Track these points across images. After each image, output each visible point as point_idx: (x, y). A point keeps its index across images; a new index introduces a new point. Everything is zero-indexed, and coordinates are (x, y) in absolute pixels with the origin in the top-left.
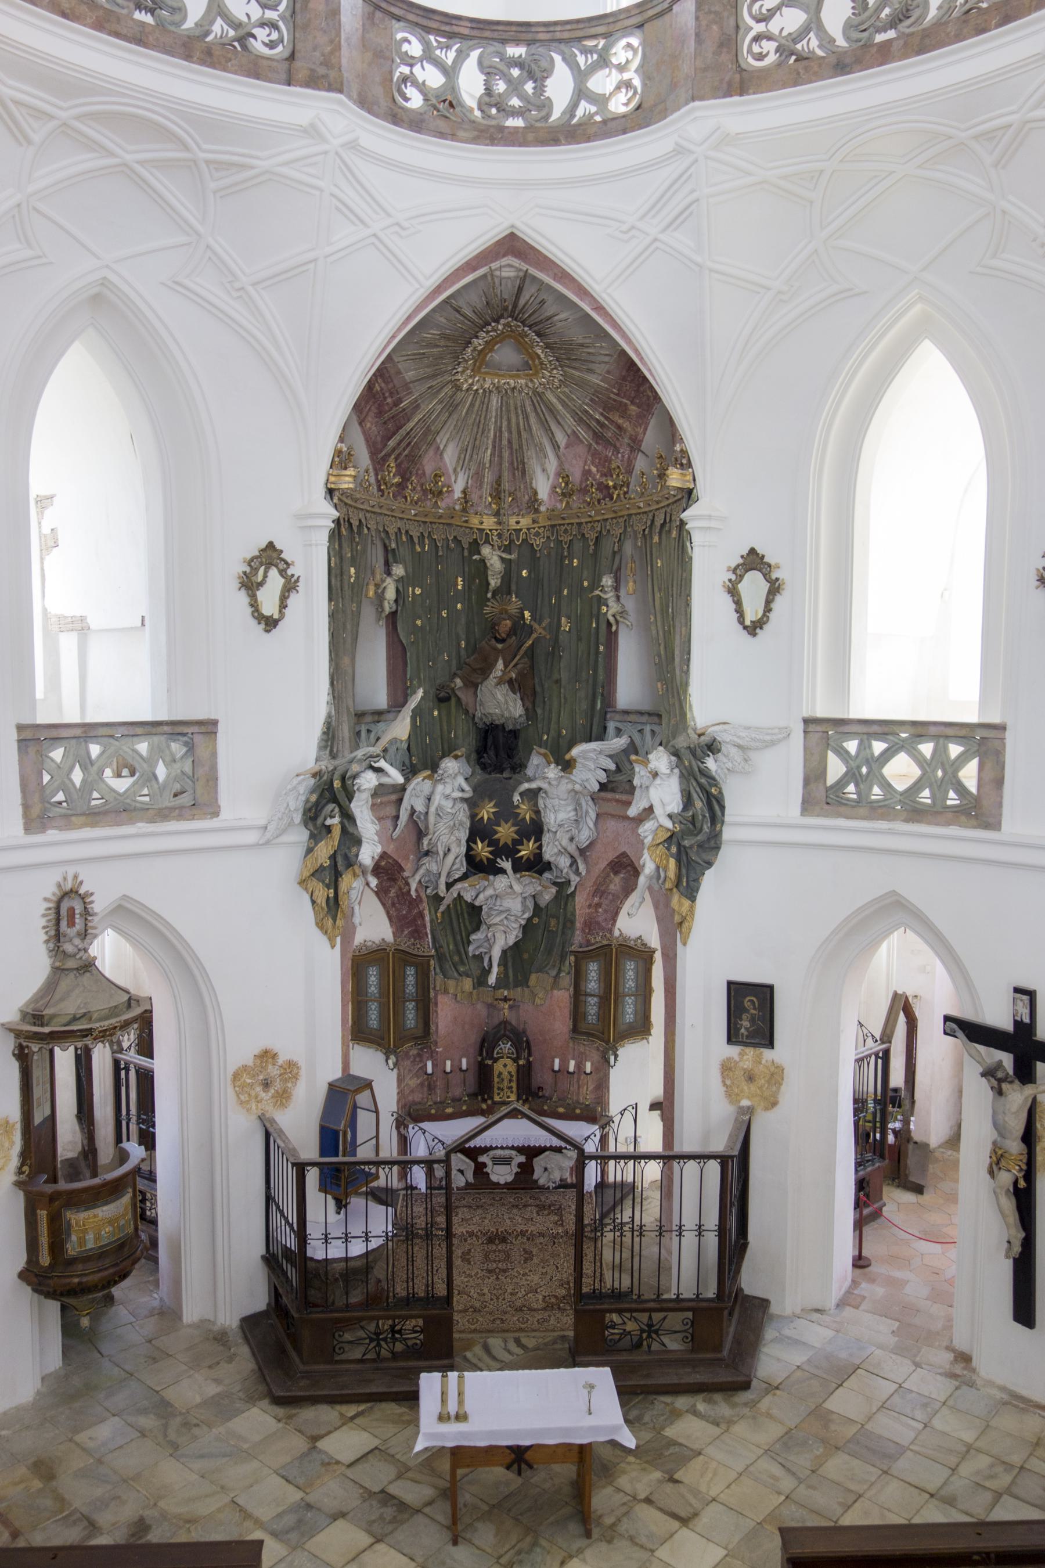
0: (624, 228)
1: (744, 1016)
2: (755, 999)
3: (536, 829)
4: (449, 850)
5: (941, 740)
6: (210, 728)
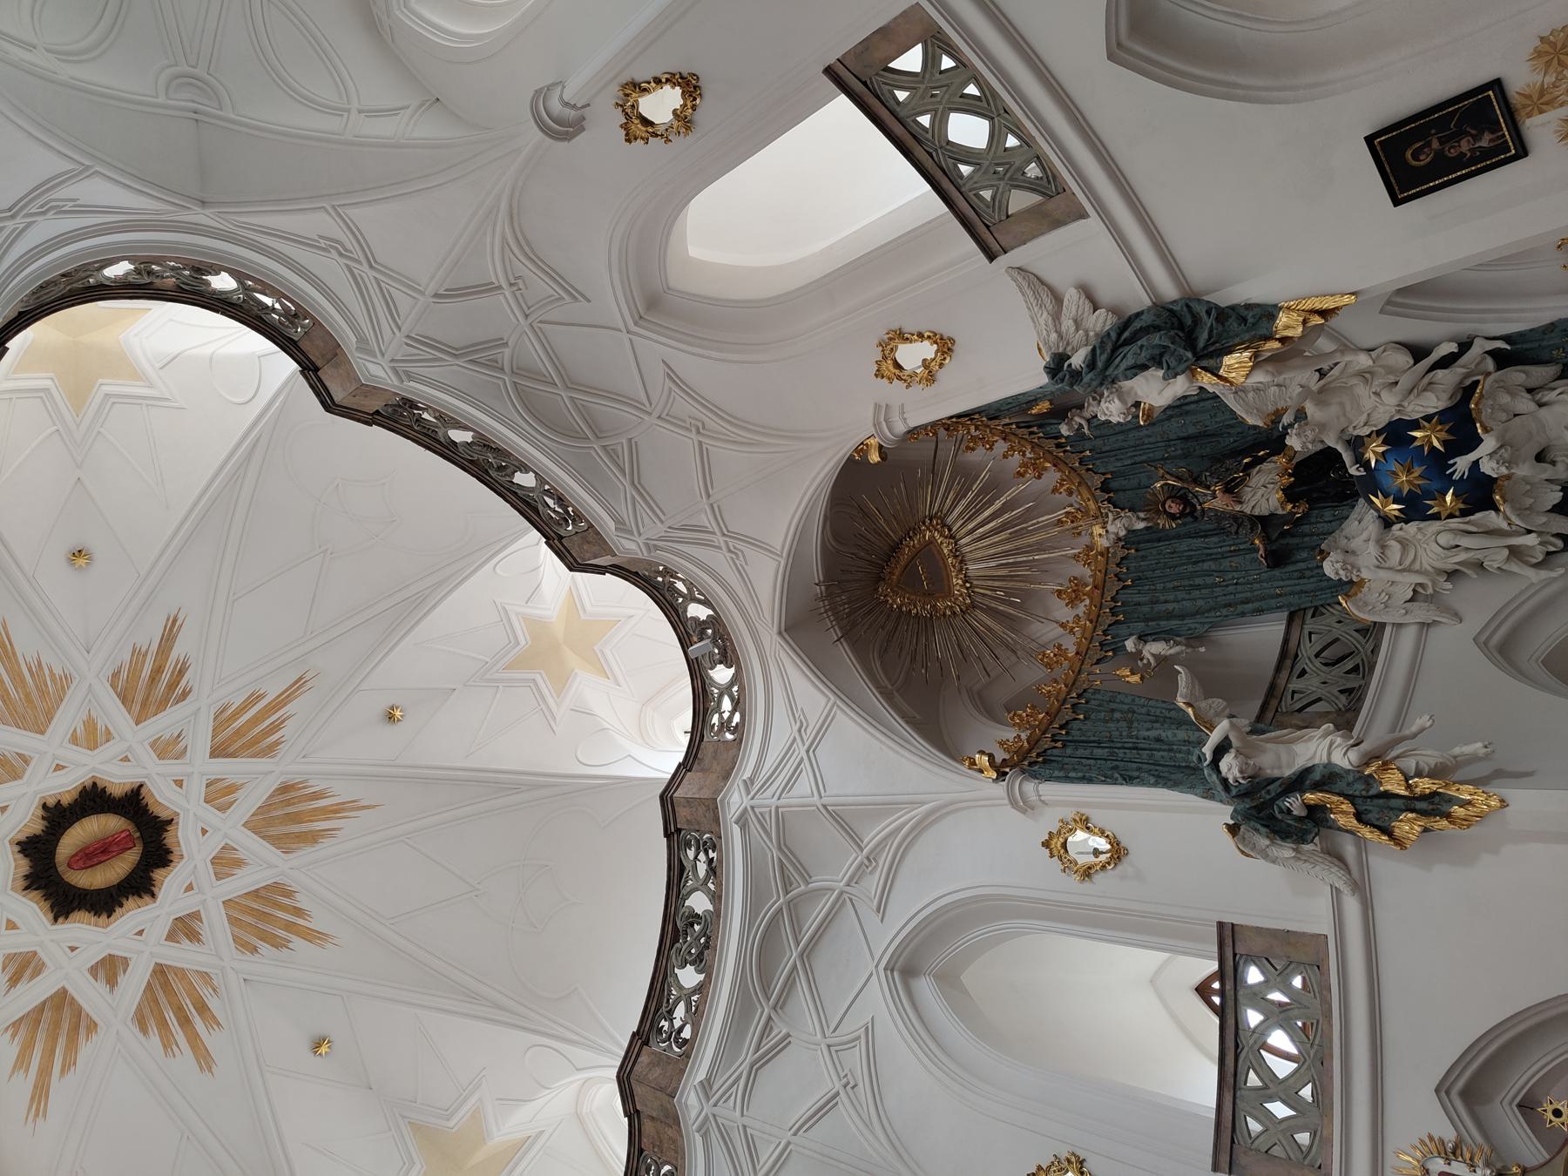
0: (734, 556)
1: (1453, 153)
2: (1409, 154)
3: (1396, 434)
4: (1457, 546)
5: (902, 113)
6: (1228, 933)
